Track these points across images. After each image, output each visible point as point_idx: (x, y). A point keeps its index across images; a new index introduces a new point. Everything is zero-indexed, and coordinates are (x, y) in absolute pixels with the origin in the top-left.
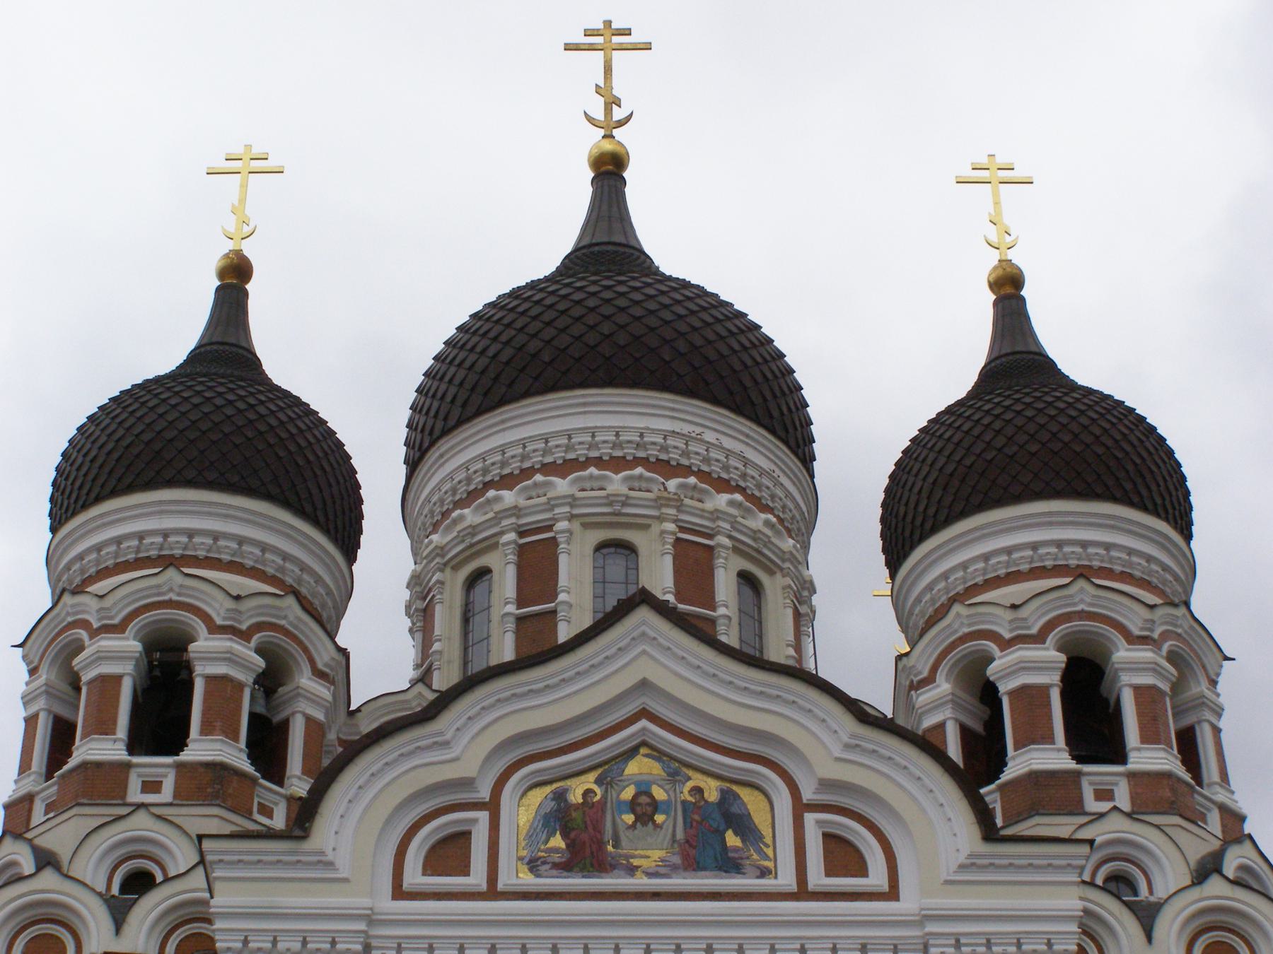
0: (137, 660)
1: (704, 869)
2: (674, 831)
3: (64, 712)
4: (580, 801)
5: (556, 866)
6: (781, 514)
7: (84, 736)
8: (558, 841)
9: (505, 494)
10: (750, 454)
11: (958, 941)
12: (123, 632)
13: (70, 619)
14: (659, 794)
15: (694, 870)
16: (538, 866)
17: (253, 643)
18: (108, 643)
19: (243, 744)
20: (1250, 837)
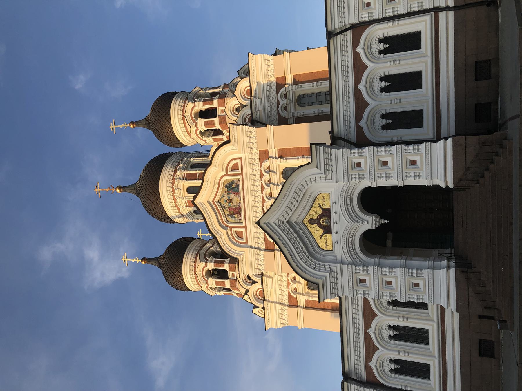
0: (212, 278)
5: (240, 216)
8: (236, 216)
9: (180, 210)
12: (208, 281)
13: (206, 289)
14: (227, 198)
19: (225, 260)
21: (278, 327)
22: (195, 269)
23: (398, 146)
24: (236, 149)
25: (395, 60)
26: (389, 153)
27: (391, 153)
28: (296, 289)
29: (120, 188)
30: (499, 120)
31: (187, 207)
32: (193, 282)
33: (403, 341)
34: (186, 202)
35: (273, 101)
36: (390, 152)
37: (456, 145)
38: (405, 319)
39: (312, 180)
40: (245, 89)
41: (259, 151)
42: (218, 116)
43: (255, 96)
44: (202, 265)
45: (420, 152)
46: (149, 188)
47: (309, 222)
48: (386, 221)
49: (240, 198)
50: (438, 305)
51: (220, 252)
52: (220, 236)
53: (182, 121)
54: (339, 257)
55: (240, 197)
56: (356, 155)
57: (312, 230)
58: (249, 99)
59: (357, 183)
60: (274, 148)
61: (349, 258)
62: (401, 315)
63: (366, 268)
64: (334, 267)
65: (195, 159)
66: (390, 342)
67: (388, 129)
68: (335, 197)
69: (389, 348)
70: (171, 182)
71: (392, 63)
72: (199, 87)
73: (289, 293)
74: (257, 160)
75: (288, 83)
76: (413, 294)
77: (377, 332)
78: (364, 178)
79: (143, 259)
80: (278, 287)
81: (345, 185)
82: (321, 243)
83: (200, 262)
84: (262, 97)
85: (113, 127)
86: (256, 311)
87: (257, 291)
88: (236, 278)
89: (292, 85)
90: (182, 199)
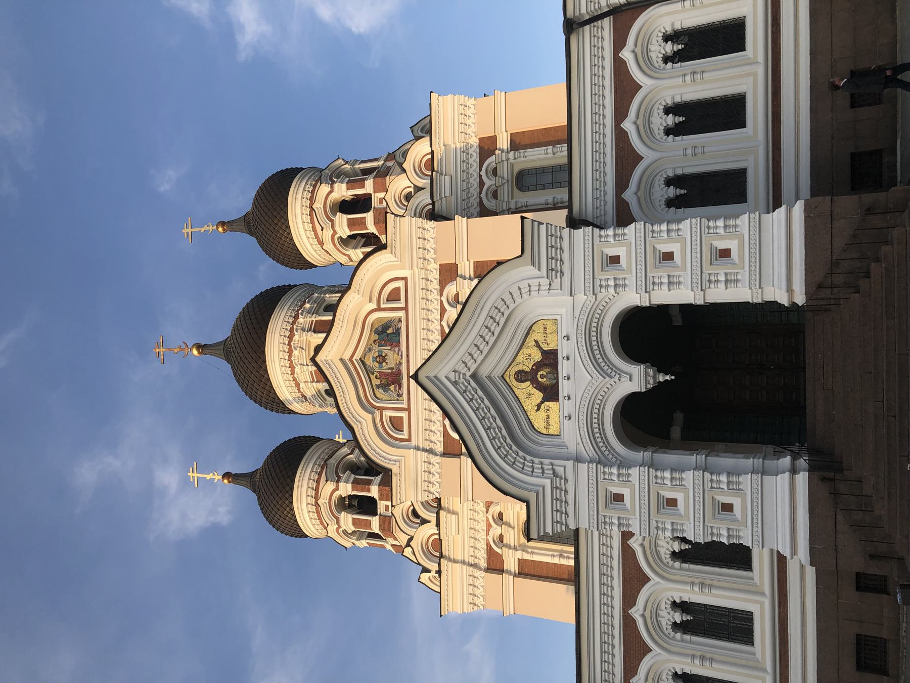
3: (366, 535)
4: (379, 380)
5: (400, 389)
7: (372, 530)
8: (392, 388)
13: (336, 533)
14: (376, 355)
17: (342, 476)
18: (342, 523)
19: (373, 478)
20: (393, 153)
21: (465, 611)
22: (317, 494)
23: (694, 220)
24: (397, 260)
25: (694, 73)
26: (676, 235)
27: (679, 234)
28: (501, 537)
29: (199, 347)
30: (899, 183)
31: (314, 381)
32: (311, 518)
33: (701, 635)
34: (311, 372)
35: (471, 181)
36: (678, 233)
37: (812, 215)
38: (705, 589)
39: (523, 291)
40: (422, 159)
41: (440, 265)
42: (372, 209)
43: (440, 171)
44: (331, 486)
45: (739, 232)
46: (247, 345)
47: (515, 378)
48: (668, 378)
49: (400, 354)
50: (772, 550)
51: (366, 464)
52: (359, 424)
53: (309, 217)
54: (572, 448)
55: (402, 352)
56: (611, 239)
57: (521, 394)
58: (429, 177)
59: (612, 297)
60: (468, 260)
61: (592, 449)
62: (697, 581)
63: (624, 471)
64: (560, 467)
65: (334, 295)
66: (674, 637)
67: (678, 207)
68: (567, 327)
69: (672, 649)
70: (287, 335)
71: (688, 78)
72: (343, 159)
73: (488, 545)
74: (435, 281)
75: (500, 148)
76: (719, 526)
77: (647, 614)
78: (625, 286)
79: (227, 475)
80: (468, 533)
81: (588, 302)
82: (538, 419)
83: (327, 481)
84: (453, 173)
85: (188, 230)
86: (425, 577)
87: (429, 538)
88: (391, 514)
89: (508, 152)
90: (304, 367)
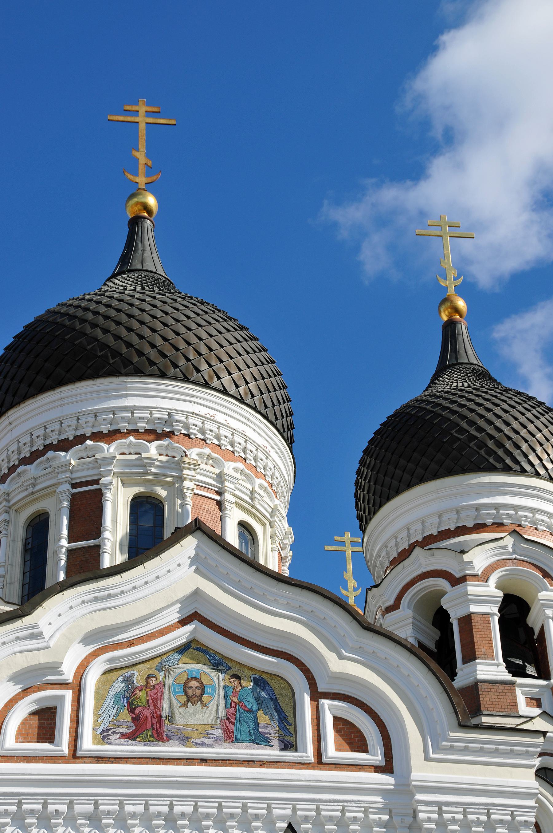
1: (242, 741)
2: (217, 710)
4: (143, 683)
5: (123, 736)
6: (270, 480)
8: (126, 717)
10: (250, 433)
11: (440, 809)
15: (232, 741)
16: (110, 735)
34: (97, 482)
49: (207, 741)
